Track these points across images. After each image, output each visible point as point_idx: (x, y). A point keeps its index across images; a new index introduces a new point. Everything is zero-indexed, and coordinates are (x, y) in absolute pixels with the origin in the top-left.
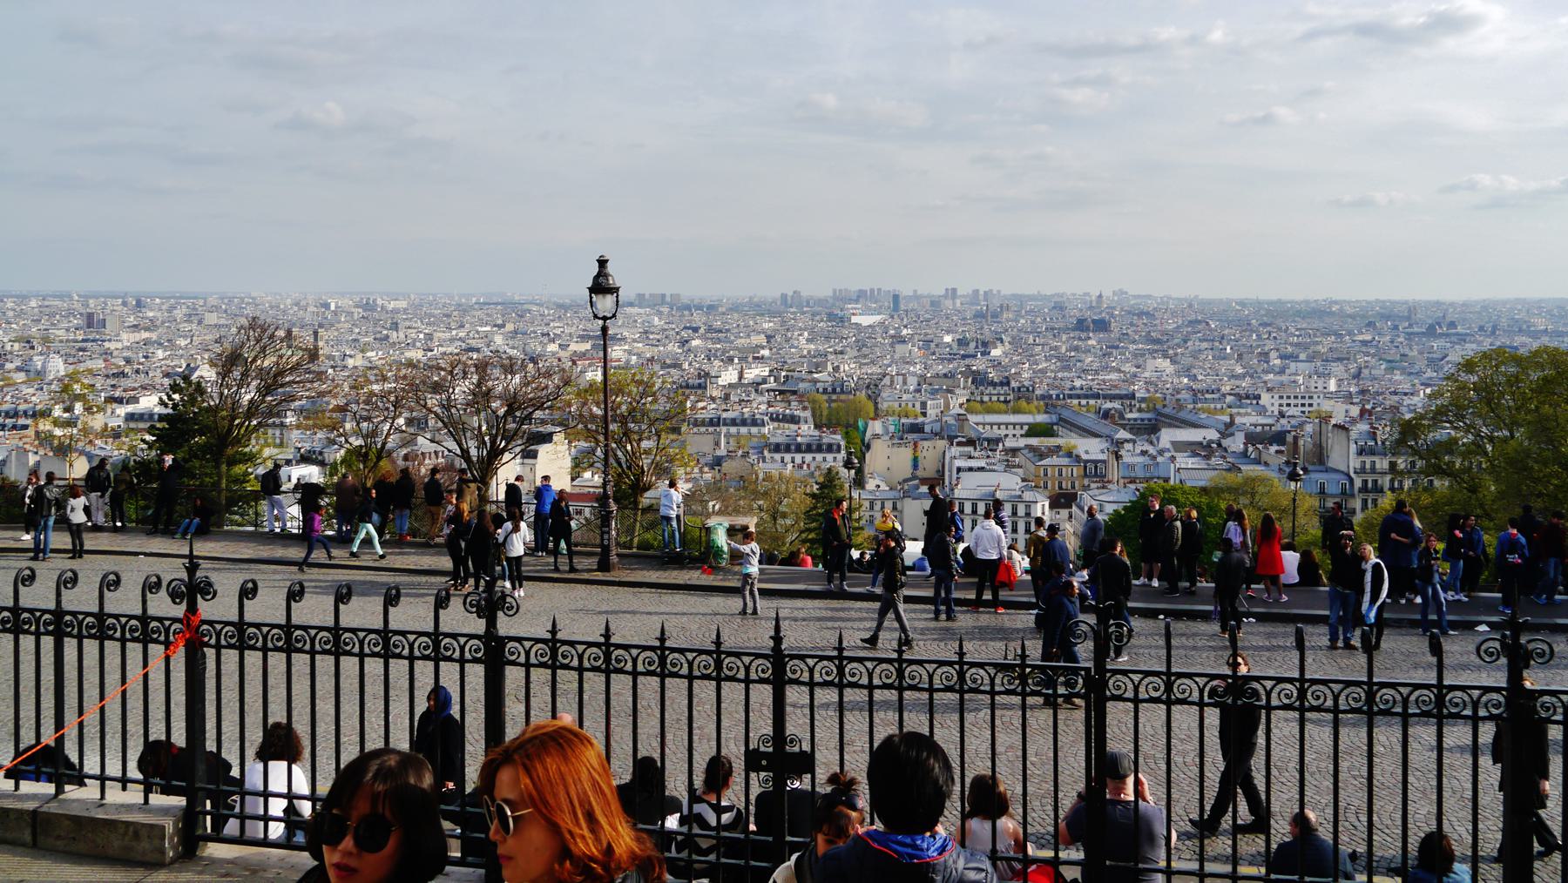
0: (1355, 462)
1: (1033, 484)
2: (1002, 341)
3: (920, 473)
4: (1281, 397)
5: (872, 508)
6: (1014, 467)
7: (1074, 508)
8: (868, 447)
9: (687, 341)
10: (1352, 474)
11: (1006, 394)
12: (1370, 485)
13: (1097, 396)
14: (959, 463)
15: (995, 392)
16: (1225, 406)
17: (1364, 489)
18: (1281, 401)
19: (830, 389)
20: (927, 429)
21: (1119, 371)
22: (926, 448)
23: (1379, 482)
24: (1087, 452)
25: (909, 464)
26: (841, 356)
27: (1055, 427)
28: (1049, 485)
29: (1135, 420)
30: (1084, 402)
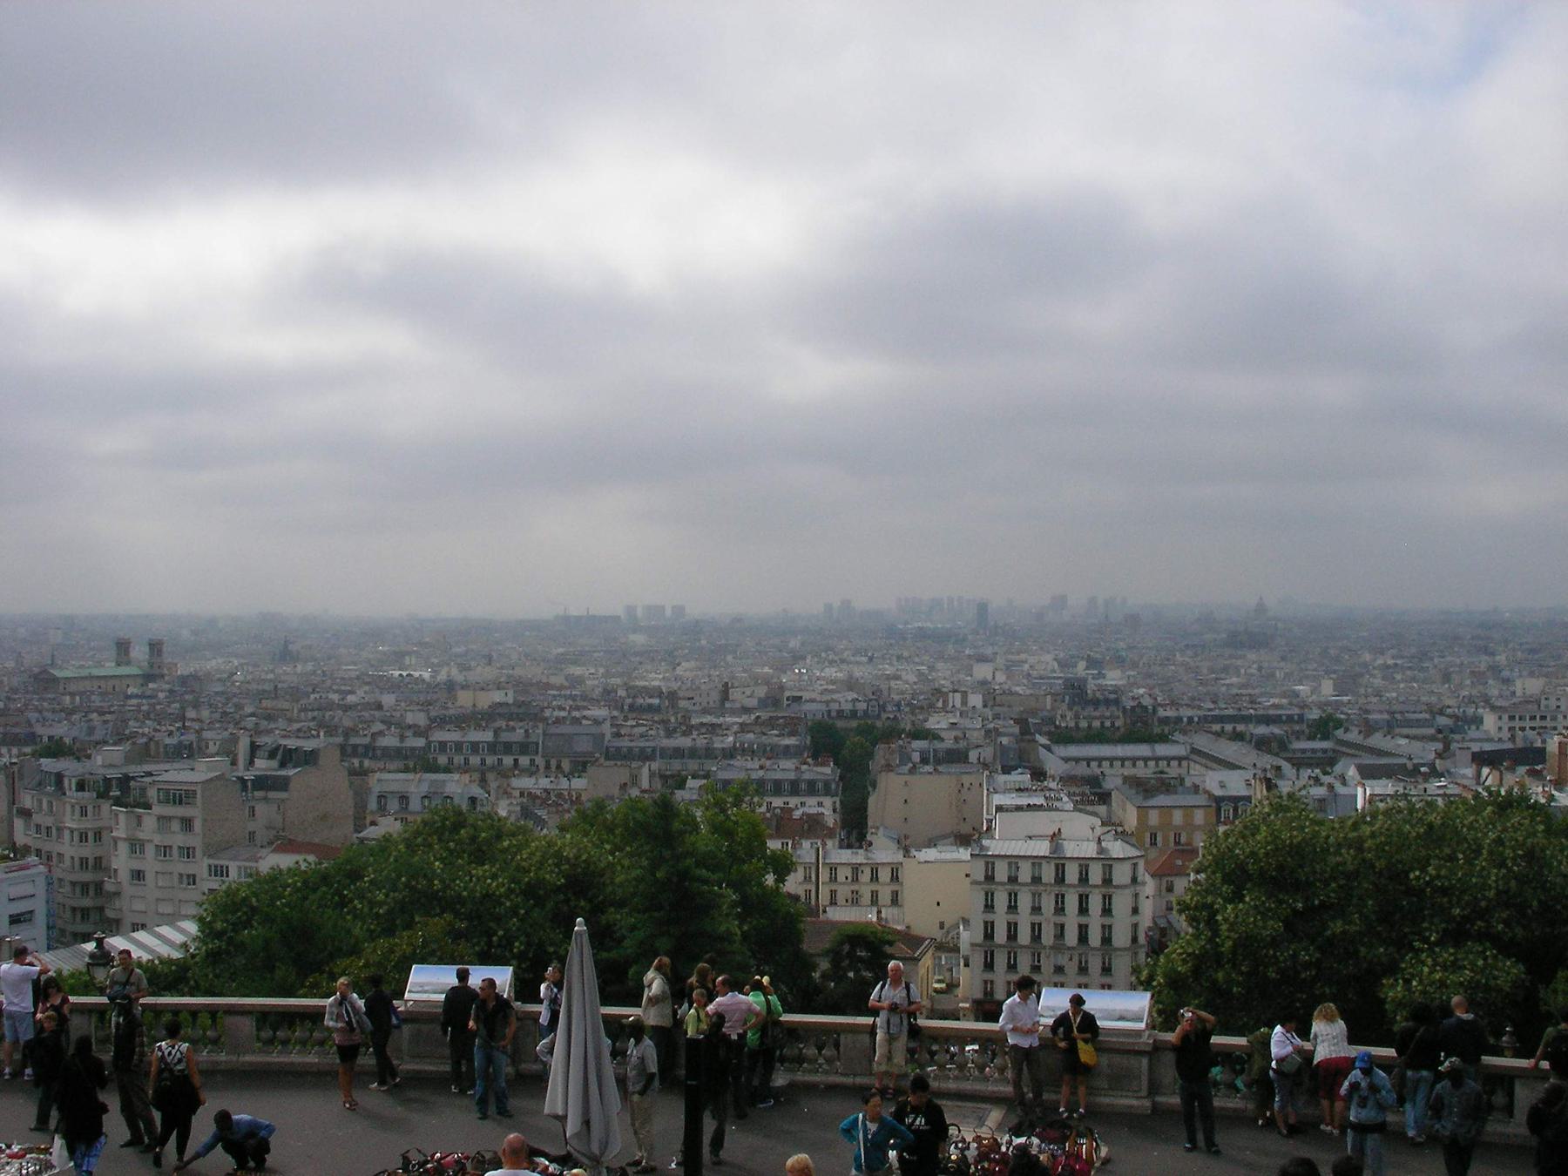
1: (1120, 829)
2: (1123, 661)
5: (856, 879)
6: (1092, 803)
8: (874, 787)
9: (679, 665)
13: (1246, 719)
14: (998, 799)
15: (1097, 714)
18: (1512, 724)
20: (973, 756)
21: (1285, 698)
22: (967, 785)
24: (1223, 786)
26: (893, 683)
27: (1184, 763)
28: (1159, 839)
29: (1304, 751)
30: (1229, 727)
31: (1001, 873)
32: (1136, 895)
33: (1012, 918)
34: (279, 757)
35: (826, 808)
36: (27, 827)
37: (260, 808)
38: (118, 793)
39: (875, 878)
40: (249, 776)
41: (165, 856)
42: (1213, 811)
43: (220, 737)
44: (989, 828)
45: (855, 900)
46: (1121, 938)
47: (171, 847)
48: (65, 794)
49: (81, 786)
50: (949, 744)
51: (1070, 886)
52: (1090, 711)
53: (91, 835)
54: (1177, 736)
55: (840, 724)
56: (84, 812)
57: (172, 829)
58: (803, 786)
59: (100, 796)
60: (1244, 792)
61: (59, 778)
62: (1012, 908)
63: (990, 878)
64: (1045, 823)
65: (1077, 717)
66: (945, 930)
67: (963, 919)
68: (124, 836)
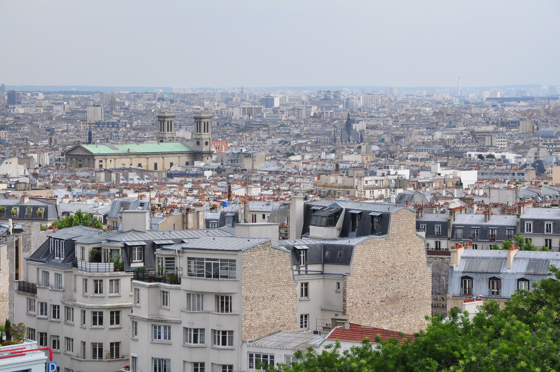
34: (340, 223)
36: (31, 307)
37: (315, 286)
38: (142, 265)
40: (302, 244)
41: (195, 341)
43: (269, 208)
47: (203, 330)
48: (75, 265)
49: (96, 257)
53: (107, 317)
56: (98, 289)
57: (205, 309)
59: (119, 267)
61: (70, 245)
68: (146, 317)
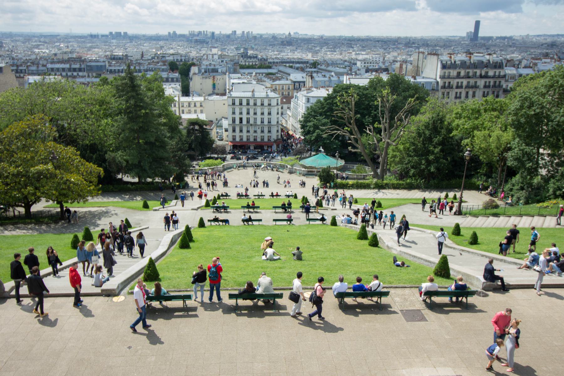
0: (439, 72)
3: (216, 91)
4: (365, 63)
5: (189, 106)
6: (262, 81)
7: (292, 103)
8: (192, 78)
10: (439, 80)
11: (255, 62)
12: (447, 84)
14: (232, 81)
15: (251, 61)
16: (344, 66)
17: (444, 87)
18: (365, 65)
19: (179, 60)
20: (220, 71)
22: (219, 79)
23: (451, 83)
25: (211, 87)
30: (288, 65)
31: (237, 102)
32: (278, 109)
33: (241, 116)
35: (178, 86)
39: (195, 106)
42: (293, 85)
44: (232, 89)
45: (189, 112)
46: (274, 122)
50: (212, 67)
51: (259, 106)
52: (249, 60)
54: (274, 67)
55: (178, 63)
58: (170, 80)
60: (302, 80)
62: (241, 113)
63: (234, 104)
64: (249, 87)
65: (245, 61)
66: (217, 121)
67: (223, 117)
